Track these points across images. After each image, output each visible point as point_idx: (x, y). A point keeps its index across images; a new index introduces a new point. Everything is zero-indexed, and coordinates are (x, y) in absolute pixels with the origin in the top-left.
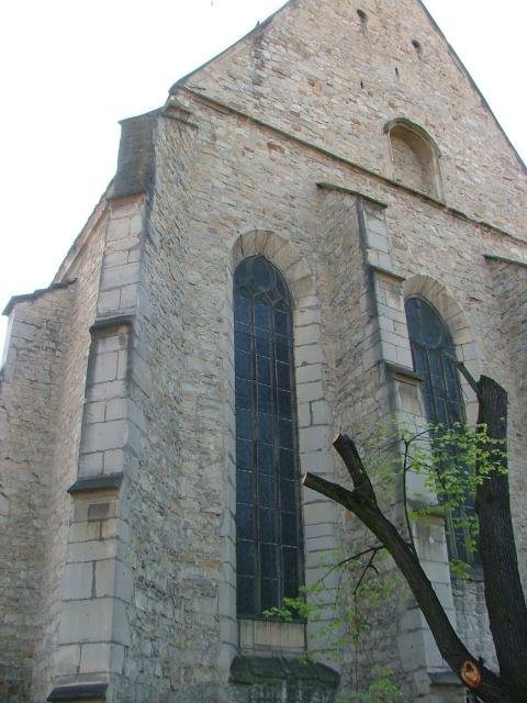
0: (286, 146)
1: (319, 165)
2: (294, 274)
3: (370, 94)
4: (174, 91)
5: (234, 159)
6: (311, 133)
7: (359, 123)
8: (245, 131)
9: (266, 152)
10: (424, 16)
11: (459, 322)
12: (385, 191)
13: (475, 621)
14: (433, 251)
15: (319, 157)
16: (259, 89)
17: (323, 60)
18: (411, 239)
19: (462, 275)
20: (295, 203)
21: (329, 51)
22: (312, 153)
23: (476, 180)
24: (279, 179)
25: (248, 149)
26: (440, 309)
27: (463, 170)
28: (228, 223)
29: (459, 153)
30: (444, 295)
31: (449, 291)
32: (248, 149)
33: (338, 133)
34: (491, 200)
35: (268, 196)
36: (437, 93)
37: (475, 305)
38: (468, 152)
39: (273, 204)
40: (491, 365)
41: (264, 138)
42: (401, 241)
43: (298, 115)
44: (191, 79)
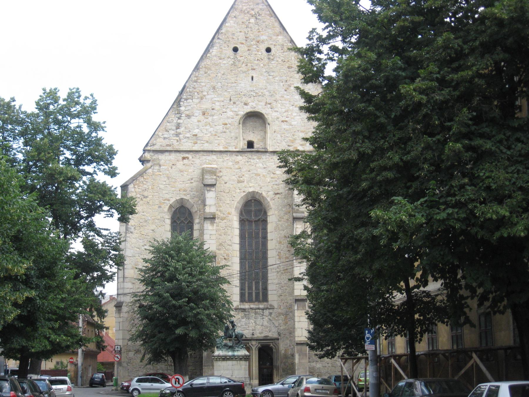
0: (190, 156)
1: (204, 157)
2: (193, 210)
3: (234, 103)
4: (145, 151)
5: (168, 172)
6: (202, 142)
7: (226, 124)
8: (173, 157)
9: (182, 163)
10: (277, 24)
11: (269, 206)
12: (237, 156)
13: (253, 321)
14: (258, 178)
15: (205, 154)
16: (178, 130)
17: (212, 96)
18: (247, 176)
19: (273, 183)
20: (192, 181)
21: (214, 88)
22: (202, 153)
23: (293, 123)
24: (186, 173)
25: (173, 165)
26: (262, 201)
27: (286, 121)
28: (165, 201)
29: (285, 112)
30: (262, 196)
31: (264, 194)
32: (173, 165)
33: (216, 135)
34: (302, 132)
35: (181, 183)
36: (277, 78)
37: (278, 196)
38: (291, 108)
39: (183, 185)
40: (280, 223)
41: (180, 156)
42: (242, 179)
43: (196, 135)
44: (150, 142)
